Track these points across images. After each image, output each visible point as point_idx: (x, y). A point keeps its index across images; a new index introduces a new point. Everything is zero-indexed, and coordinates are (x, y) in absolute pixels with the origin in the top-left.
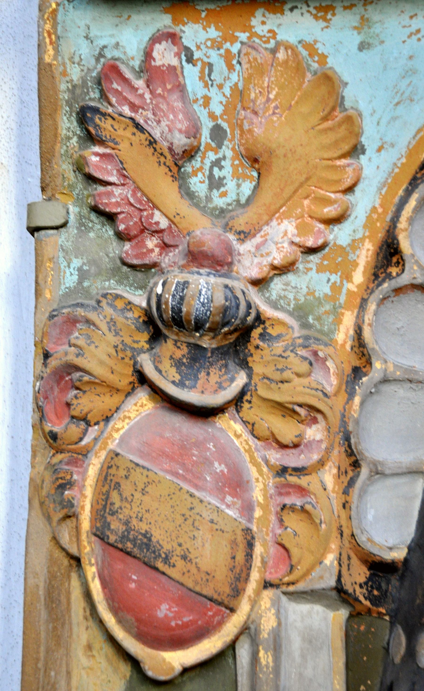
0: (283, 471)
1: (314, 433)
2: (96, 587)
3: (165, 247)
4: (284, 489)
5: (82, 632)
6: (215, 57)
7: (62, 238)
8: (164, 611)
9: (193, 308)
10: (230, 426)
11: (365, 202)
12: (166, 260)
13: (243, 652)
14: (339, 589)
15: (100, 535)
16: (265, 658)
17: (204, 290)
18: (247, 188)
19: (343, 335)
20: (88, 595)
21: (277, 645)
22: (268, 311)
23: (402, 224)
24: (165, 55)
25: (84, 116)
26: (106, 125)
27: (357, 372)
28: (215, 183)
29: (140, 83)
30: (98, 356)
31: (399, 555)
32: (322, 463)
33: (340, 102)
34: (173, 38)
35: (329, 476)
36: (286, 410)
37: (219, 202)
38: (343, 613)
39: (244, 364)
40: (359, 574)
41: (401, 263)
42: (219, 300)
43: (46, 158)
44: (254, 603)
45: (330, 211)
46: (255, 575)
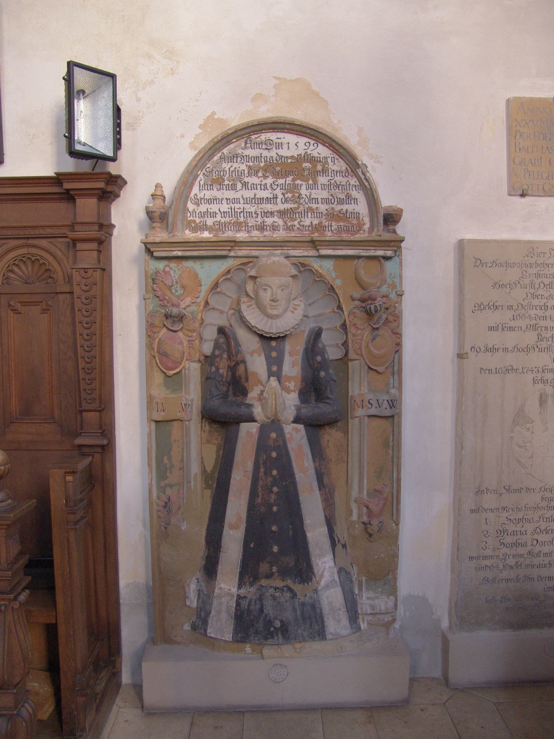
0: (189, 341)
1: (194, 334)
2: (158, 361)
3: (168, 302)
4: (190, 344)
5: (156, 369)
6: (176, 269)
7: (150, 301)
8: (170, 364)
9: (173, 314)
10: (180, 334)
11: (202, 294)
12: (168, 305)
13: (183, 371)
14: (199, 360)
15: (158, 352)
16: (187, 372)
17: (175, 311)
18: (182, 292)
19: (199, 317)
20: (156, 363)
21: (189, 369)
22: (185, 313)
23: (209, 298)
24: (167, 269)
25: (153, 280)
26: (157, 281)
27: (202, 324)
28: (177, 291)
29: (163, 274)
30: (157, 322)
31: (209, 354)
32: (196, 339)
33: (198, 277)
34: (169, 266)
35: (197, 342)
36: (189, 331)
37: (177, 294)
38: (200, 364)
39: (182, 323)
40: (202, 358)
41: (209, 305)
42: (178, 313)
43: (146, 286)
44: (185, 363)
45: (196, 296)
46: (185, 358)
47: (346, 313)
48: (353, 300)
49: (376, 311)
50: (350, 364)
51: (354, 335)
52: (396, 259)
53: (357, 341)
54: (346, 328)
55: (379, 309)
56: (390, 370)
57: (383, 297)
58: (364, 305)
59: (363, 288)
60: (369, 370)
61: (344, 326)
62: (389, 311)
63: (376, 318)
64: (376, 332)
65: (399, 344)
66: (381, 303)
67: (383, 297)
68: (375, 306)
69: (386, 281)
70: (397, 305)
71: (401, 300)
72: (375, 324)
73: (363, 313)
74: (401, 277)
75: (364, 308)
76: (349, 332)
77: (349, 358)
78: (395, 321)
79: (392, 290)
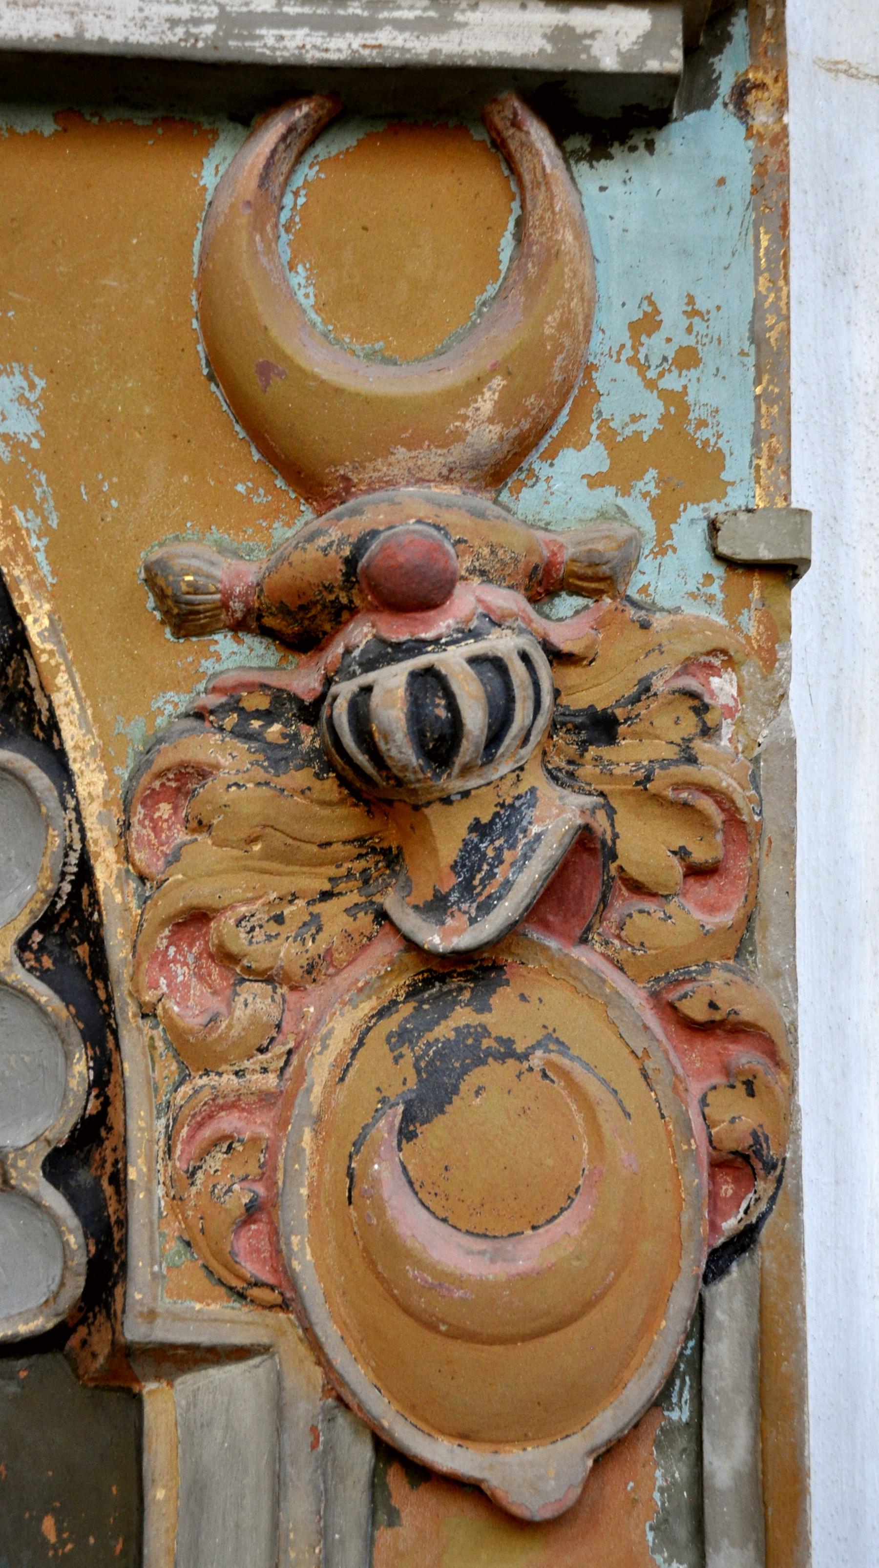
47: (91, 781)
48: (187, 618)
49: (440, 743)
50: (164, 1404)
51: (192, 1053)
52: (708, 137)
53: (228, 1122)
54: (99, 965)
55: (475, 718)
56: (658, 1477)
57: (545, 584)
58: (304, 680)
59: (311, 481)
60: (395, 1479)
61: (67, 931)
62: (628, 754)
63: (449, 832)
64: (463, 1016)
65: (753, 1163)
66: (503, 643)
67: (545, 584)
68: (430, 680)
69: (590, 394)
70: (723, 687)
71: (778, 629)
72: (437, 907)
73: (301, 778)
74: (770, 355)
75: (311, 711)
76: (127, 1012)
77: (135, 1331)
78: (699, 872)
79: (665, 511)
